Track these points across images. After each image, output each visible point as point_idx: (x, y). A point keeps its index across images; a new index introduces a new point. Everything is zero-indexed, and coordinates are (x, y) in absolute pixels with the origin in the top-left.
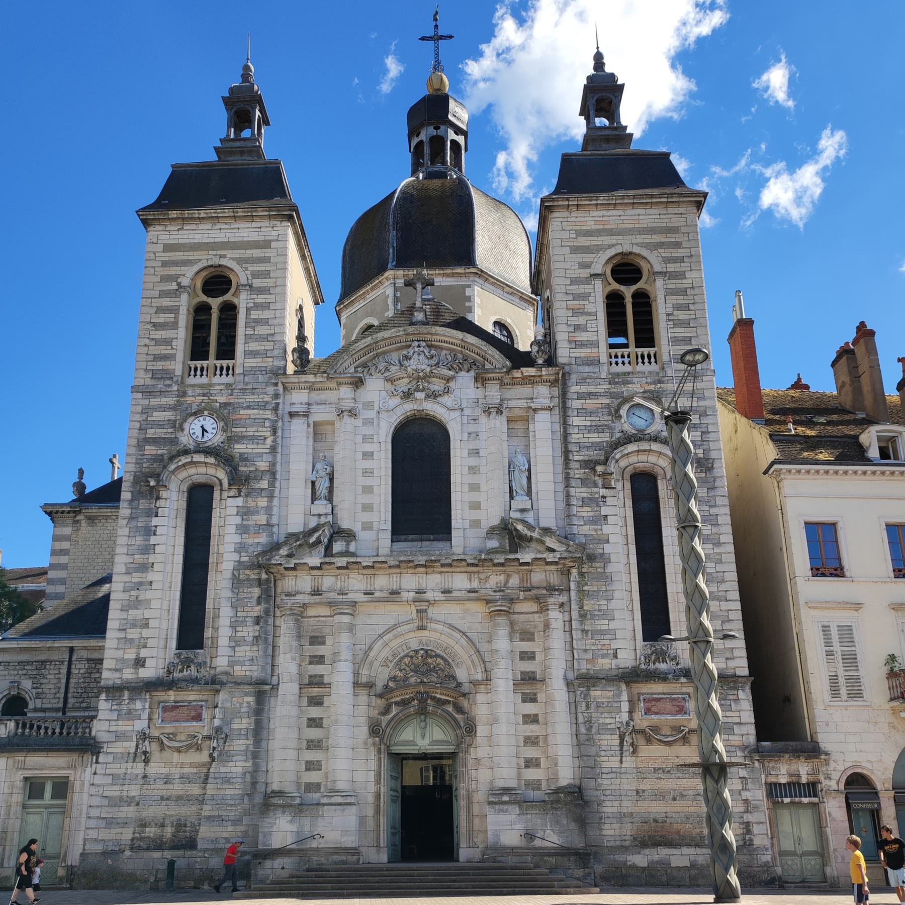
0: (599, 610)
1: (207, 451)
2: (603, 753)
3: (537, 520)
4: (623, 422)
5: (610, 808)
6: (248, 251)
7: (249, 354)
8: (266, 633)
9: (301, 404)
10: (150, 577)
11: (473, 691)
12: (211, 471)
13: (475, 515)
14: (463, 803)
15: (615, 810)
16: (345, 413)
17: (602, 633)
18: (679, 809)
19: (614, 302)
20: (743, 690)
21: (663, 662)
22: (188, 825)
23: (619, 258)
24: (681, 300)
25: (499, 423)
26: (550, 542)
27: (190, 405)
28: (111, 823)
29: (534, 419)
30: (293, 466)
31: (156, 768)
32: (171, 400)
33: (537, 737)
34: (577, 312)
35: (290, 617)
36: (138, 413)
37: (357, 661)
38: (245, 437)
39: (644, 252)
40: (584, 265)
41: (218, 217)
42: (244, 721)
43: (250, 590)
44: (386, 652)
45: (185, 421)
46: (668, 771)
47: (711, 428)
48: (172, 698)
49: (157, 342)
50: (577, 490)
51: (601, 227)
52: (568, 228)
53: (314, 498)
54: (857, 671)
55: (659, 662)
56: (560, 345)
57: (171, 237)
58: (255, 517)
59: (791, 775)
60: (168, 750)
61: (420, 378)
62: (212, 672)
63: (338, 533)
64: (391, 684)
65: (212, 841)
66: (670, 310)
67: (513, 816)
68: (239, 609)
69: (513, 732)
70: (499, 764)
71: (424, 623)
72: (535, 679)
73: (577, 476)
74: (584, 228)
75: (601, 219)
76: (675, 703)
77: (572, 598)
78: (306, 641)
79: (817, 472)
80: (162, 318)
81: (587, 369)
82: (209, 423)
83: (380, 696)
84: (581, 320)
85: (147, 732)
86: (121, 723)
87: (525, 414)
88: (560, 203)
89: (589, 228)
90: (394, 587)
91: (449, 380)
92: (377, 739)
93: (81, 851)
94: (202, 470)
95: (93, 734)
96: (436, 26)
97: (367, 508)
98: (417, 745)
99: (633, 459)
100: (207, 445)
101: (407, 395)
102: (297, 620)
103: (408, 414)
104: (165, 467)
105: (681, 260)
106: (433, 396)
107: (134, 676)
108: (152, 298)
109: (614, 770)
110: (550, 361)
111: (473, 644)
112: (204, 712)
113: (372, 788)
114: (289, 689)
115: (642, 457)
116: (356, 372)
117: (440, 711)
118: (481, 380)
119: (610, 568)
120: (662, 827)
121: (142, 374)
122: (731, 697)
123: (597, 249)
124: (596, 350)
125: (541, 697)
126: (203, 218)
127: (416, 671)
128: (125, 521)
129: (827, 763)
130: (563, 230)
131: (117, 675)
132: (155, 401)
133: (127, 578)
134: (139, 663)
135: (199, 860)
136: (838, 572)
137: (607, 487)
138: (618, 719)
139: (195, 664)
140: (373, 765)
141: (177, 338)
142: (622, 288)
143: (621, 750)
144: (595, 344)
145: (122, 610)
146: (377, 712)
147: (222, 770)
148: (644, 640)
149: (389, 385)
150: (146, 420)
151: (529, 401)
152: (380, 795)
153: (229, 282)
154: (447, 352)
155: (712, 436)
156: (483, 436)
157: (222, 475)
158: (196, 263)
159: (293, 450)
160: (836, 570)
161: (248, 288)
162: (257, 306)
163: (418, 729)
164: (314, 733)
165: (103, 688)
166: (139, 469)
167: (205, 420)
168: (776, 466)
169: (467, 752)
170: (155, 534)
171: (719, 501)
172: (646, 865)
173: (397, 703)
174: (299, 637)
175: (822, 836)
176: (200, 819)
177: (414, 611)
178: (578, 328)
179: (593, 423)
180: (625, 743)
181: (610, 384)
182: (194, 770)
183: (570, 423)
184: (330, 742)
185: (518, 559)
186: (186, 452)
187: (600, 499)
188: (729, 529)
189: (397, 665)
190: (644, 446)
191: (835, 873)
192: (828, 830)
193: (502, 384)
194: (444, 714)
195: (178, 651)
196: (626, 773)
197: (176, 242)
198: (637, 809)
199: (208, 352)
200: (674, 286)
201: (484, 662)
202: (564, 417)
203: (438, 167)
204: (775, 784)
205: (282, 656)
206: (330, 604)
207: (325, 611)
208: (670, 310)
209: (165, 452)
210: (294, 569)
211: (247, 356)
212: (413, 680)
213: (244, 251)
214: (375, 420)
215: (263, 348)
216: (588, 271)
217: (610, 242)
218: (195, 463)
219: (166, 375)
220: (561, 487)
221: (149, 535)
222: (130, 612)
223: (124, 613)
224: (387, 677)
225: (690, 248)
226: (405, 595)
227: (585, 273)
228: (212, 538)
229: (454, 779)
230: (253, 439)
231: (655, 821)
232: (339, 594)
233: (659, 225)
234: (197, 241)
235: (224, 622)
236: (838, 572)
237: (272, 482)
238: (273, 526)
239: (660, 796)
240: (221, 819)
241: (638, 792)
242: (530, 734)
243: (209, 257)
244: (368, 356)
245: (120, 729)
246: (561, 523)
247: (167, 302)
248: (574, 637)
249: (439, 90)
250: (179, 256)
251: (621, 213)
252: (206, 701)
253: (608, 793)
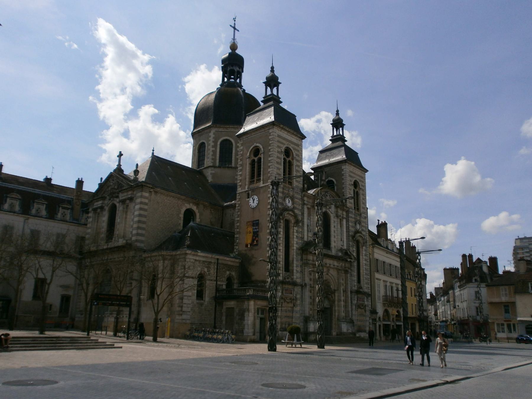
147: (296, 309)
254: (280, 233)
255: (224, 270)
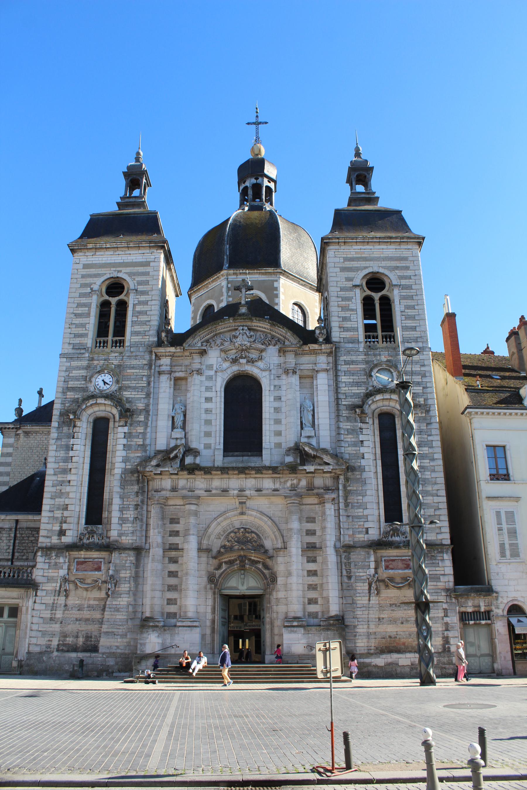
0: (357, 503)
1: (107, 397)
2: (358, 595)
3: (318, 443)
4: (373, 379)
5: (361, 629)
6: (135, 268)
7: (135, 333)
8: (142, 515)
9: (166, 365)
10: (69, 477)
11: (275, 555)
12: (108, 409)
13: (277, 439)
14: (268, 626)
15: (365, 630)
16: (195, 372)
17: (359, 517)
18: (405, 629)
19: (368, 302)
20: (447, 553)
21: (397, 536)
22: (93, 637)
23: (371, 275)
24: (410, 303)
25: (294, 380)
26: (327, 459)
27: (96, 366)
28: (45, 634)
29: (317, 377)
30: (161, 406)
31: (72, 601)
32: (85, 363)
33: (316, 585)
34: (345, 309)
35: (157, 506)
36: (63, 371)
37: (200, 535)
38: (129, 387)
39: (386, 272)
40: (349, 279)
41: (117, 247)
42: (128, 572)
43: (132, 487)
44: (219, 529)
45: (92, 377)
46: (399, 606)
47: (428, 385)
48: (83, 556)
49: (77, 326)
50: (344, 424)
51: (360, 256)
52: (339, 256)
53: (173, 427)
54: (517, 540)
55: (395, 536)
56: (334, 329)
57: (88, 259)
58: (135, 440)
59: (474, 606)
60: (80, 589)
61: (243, 350)
62: (108, 540)
63: (189, 451)
64: (222, 550)
65: (108, 648)
66: (403, 309)
67: (300, 635)
68: (125, 500)
69: (300, 581)
70: (291, 602)
71: (244, 510)
72: (315, 547)
73: (344, 415)
74: (348, 256)
75: (359, 251)
76: (404, 562)
77: (340, 495)
78: (167, 521)
79: (494, 414)
80: (80, 310)
81: (351, 345)
82: (108, 378)
83: (215, 558)
84: (347, 314)
85: (67, 577)
86: (50, 571)
87: (311, 374)
88: (334, 241)
89: (352, 256)
90: (225, 486)
91: (262, 351)
92: (213, 585)
93: (26, 651)
94: (102, 408)
95: (33, 577)
96: (257, 116)
97: (208, 434)
98: (238, 589)
99: (380, 404)
100: (105, 392)
101: (235, 361)
102: (161, 507)
103: (235, 373)
104: (79, 406)
105: (410, 278)
106: (251, 361)
107: (59, 541)
108: (74, 298)
109: (365, 605)
110: (328, 340)
111: (276, 524)
112: (102, 565)
113: (209, 616)
114: (156, 552)
115: (386, 403)
116: (202, 345)
117: (253, 568)
118: (282, 351)
119: (365, 475)
120: (394, 641)
121: (67, 346)
122: (439, 558)
123: (357, 269)
124: (356, 333)
125: (319, 559)
126: (108, 248)
127: (238, 542)
128: (54, 441)
129: (497, 598)
130: (335, 257)
131: (48, 540)
132: (75, 363)
133: (54, 478)
134: (62, 533)
135: (100, 659)
136: (506, 477)
137: (362, 422)
138: (368, 573)
139: (97, 534)
140: (210, 602)
141: (89, 323)
142: (373, 294)
143: (370, 592)
144: (356, 329)
145: (51, 498)
146: (213, 568)
147: (114, 603)
148: (386, 521)
149: (223, 355)
150: (69, 376)
151: (313, 365)
152: (214, 621)
153: (123, 287)
154: (261, 333)
155: (429, 390)
156: (284, 388)
157: (115, 411)
158: (103, 276)
159: (161, 396)
160: (505, 475)
161: (134, 291)
162: (140, 303)
163: (239, 579)
164: (173, 581)
165: (39, 548)
166: (63, 408)
167: (105, 376)
168: (468, 410)
169: (270, 594)
170: (72, 450)
171: (434, 432)
172: (383, 665)
173: (226, 563)
174: (163, 518)
175: (492, 644)
176: (100, 634)
177: (237, 503)
178: (345, 319)
179: (355, 381)
180: (372, 588)
181: (365, 355)
182: (97, 603)
183: (340, 380)
184: (183, 587)
185: (306, 470)
186: (93, 397)
187: (359, 430)
188: (439, 450)
189: (226, 538)
190: (387, 396)
191: (500, 667)
192: (496, 640)
193: (296, 354)
194: (257, 570)
195: (86, 526)
196: (372, 607)
197: (91, 262)
198: (378, 630)
199: (108, 331)
200: (405, 294)
201: (283, 536)
202: (336, 376)
203: (257, 202)
204: (465, 613)
205: (152, 531)
206: (184, 497)
207: (180, 502)
208: (403, 309)
209: (79, 396)
210: (160, 474)
211: (133, 335)
212: (236, 547)
213: (133, 268)
214: (214, 377)
215: (143, 329)
216: (351, 283)
217: (365, 265)
218: (98, 404)
219: (82, 347)
220: (333, 422)
221: (69, 450)
222: (56, 500)
223: (52, 500)
224: (219, 545)
225: (415, 270)
226: (232, 492)
227: (349, 284)
228: (108, 453)
229: (262, 612)
230: (135, 388)
231: (390, 637)
232: (188, 491)
233: (395, 255)
234: (104, 262)
235: (115, 507)
236: (506, 477)
237: (147, 418)
238: (147, 445)
239: (393, 621)
240: (114, 634)
241: (379, 619)
242: (311, 583)
243: (111, 272)
244: (210, 335)
245: (50, 574)
246: (334, 446)
247: (84, 300)
248: (341, 520)
249: (257, 155)
250: (93, 271)
251: (371, 247)
252: (104, 559)
253: (360, 620)
254: (72, 448)
255: (33, 538)
